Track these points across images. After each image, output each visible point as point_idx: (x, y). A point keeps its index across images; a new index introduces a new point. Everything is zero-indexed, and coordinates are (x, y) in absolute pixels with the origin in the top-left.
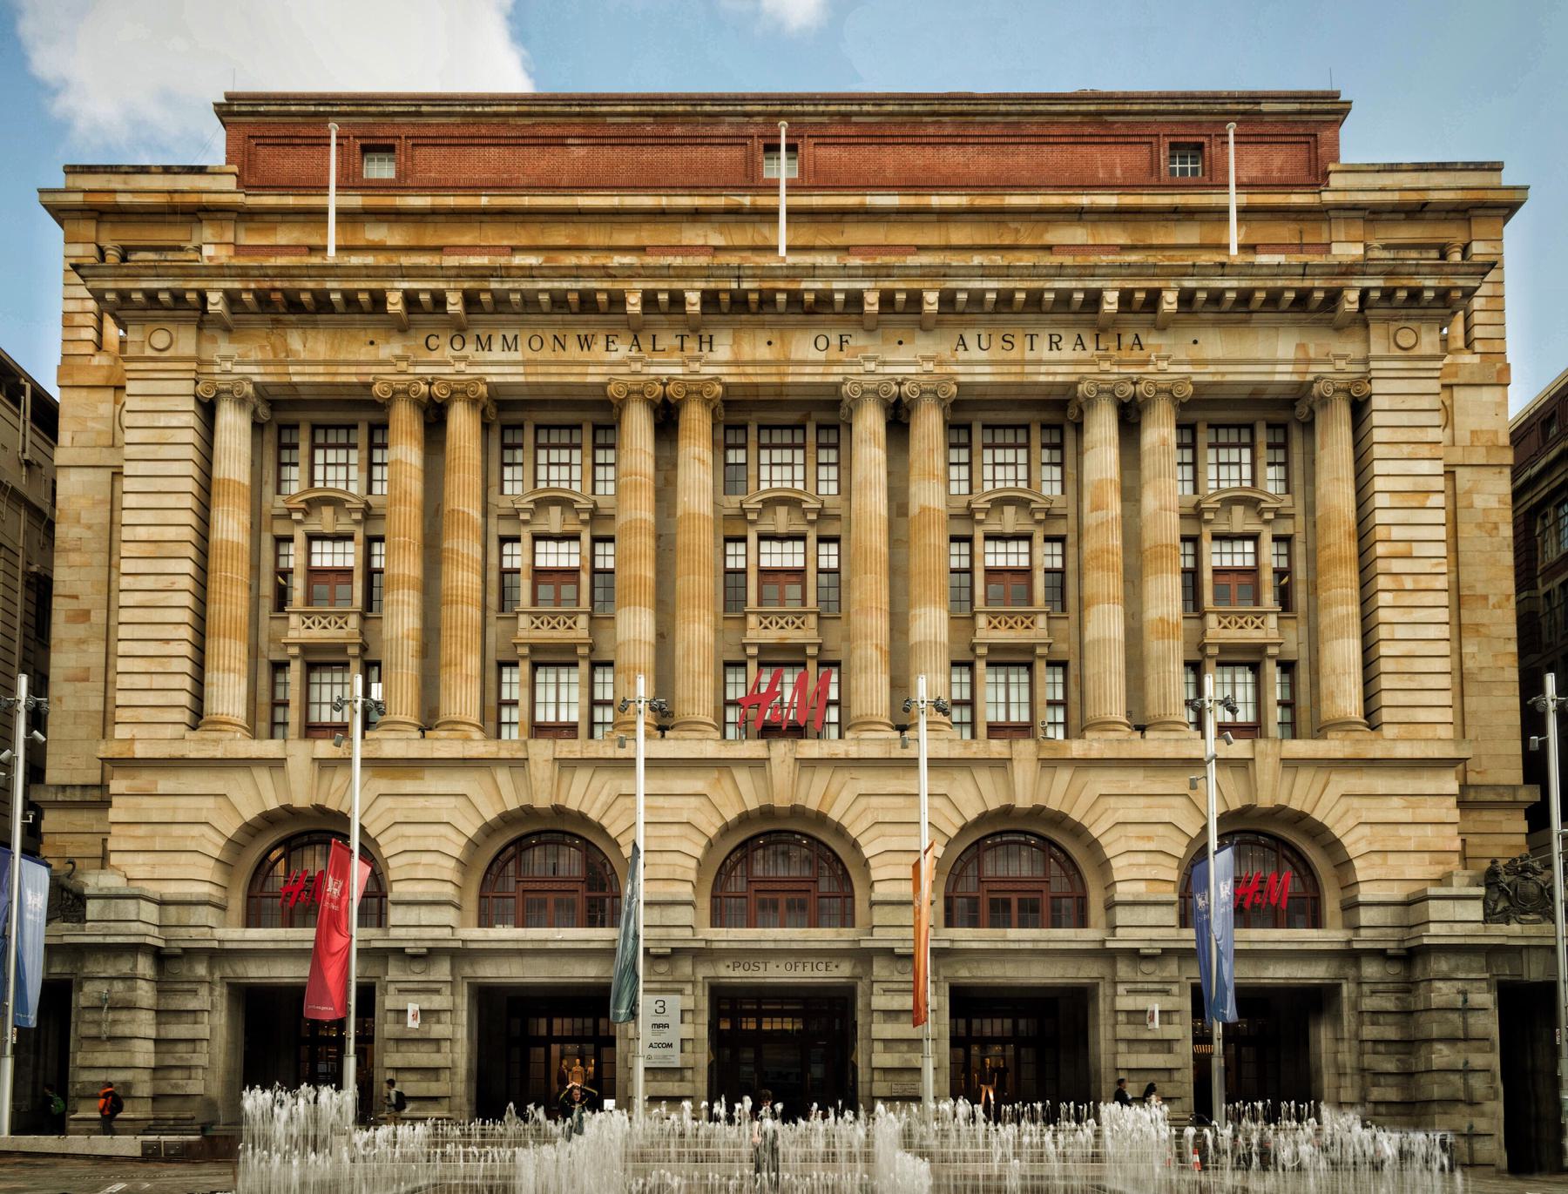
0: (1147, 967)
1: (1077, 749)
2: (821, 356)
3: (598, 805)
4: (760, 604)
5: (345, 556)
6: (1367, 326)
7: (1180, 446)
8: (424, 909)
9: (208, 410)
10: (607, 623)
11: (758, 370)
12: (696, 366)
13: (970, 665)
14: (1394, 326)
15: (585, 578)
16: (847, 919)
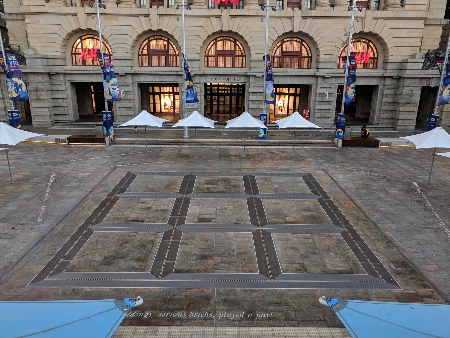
0: (326, 80)
1: (313, 13)
3: (171, 29)
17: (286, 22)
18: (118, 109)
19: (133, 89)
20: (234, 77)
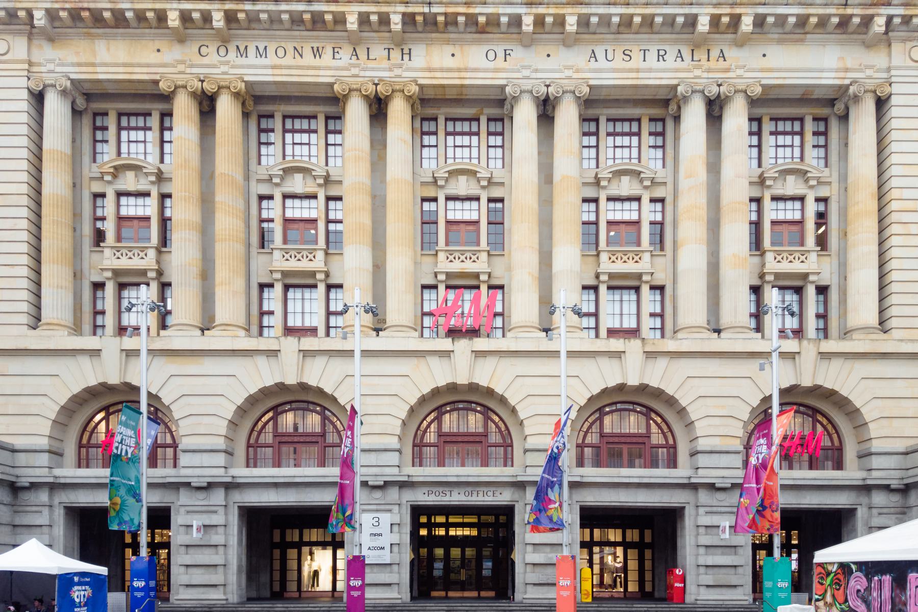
2: (491, 65)
4: (447, 244)
5: (149, 208)
6: (890, 45)
7: (751, 134)
9: (38, 98)
10: (337, 257)
11: (445, 75)
12: (397, 71)
13: (595, 289)
14: (909, 44)
15: (321, 225)
16: (508, 460)
20: (486, 490)
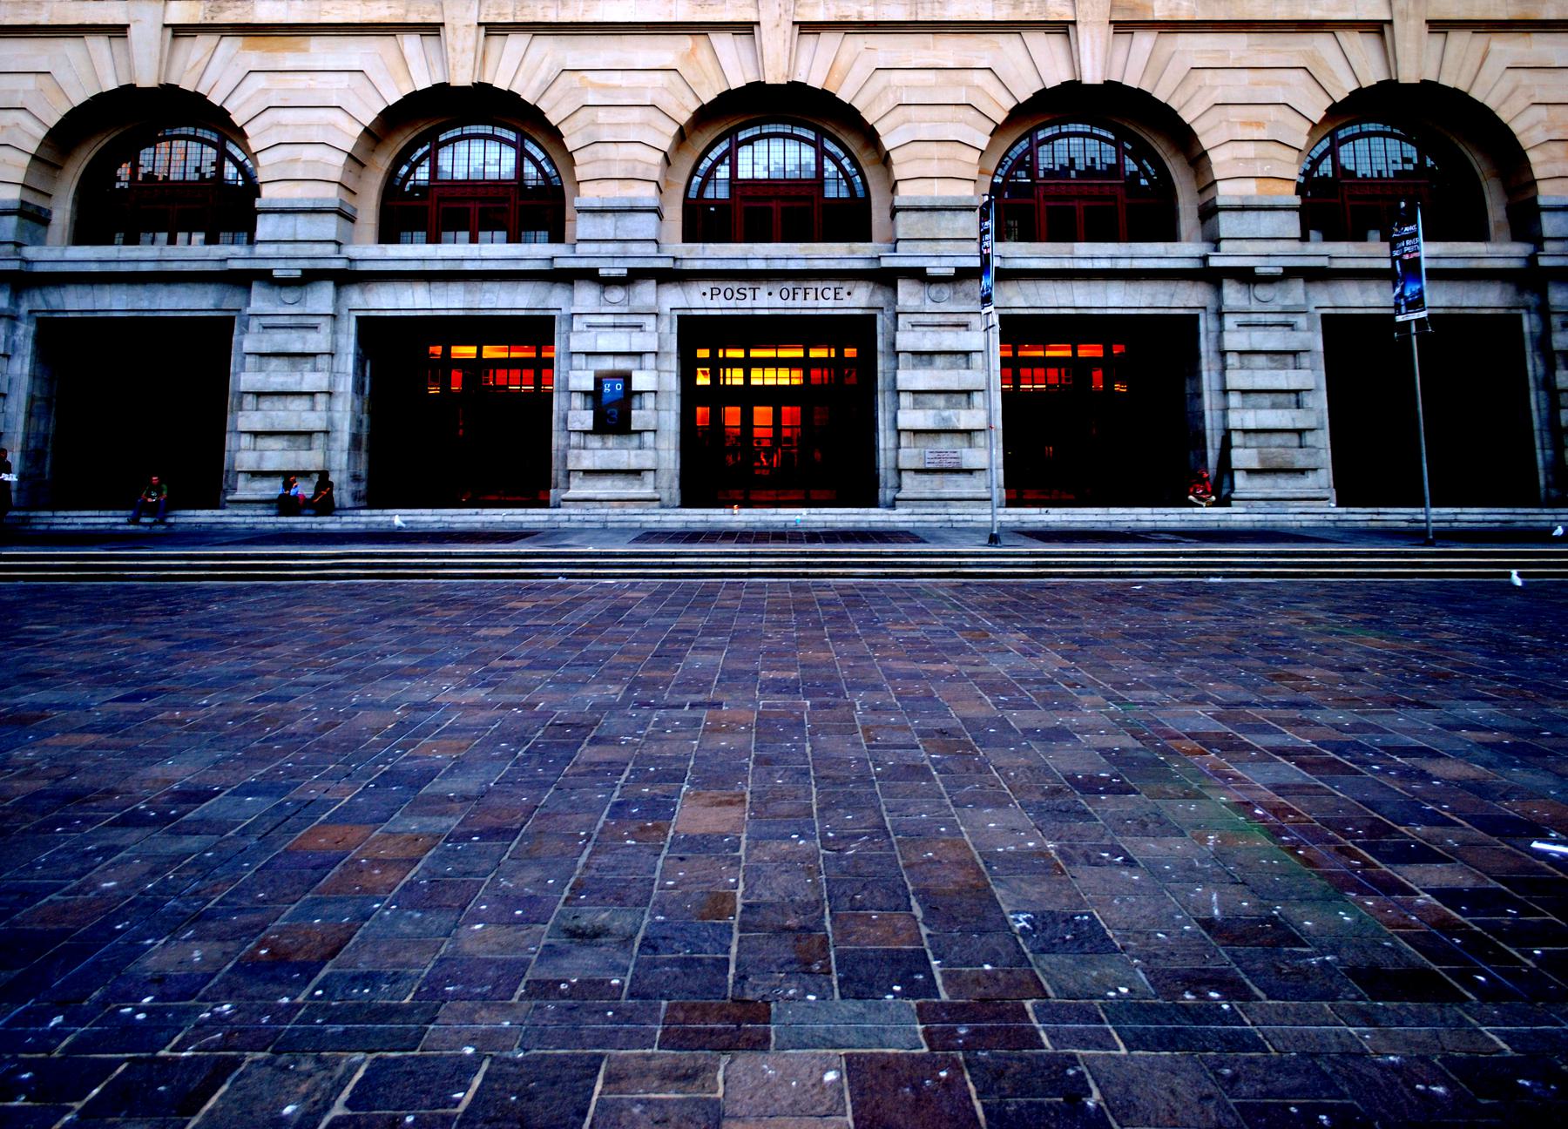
0: (1262, 291)
3: (535, 84)
8: (301, 218)
17: (1046, 47)
18: (246, 441)
19: (335, 343)
20: (820, 285)
